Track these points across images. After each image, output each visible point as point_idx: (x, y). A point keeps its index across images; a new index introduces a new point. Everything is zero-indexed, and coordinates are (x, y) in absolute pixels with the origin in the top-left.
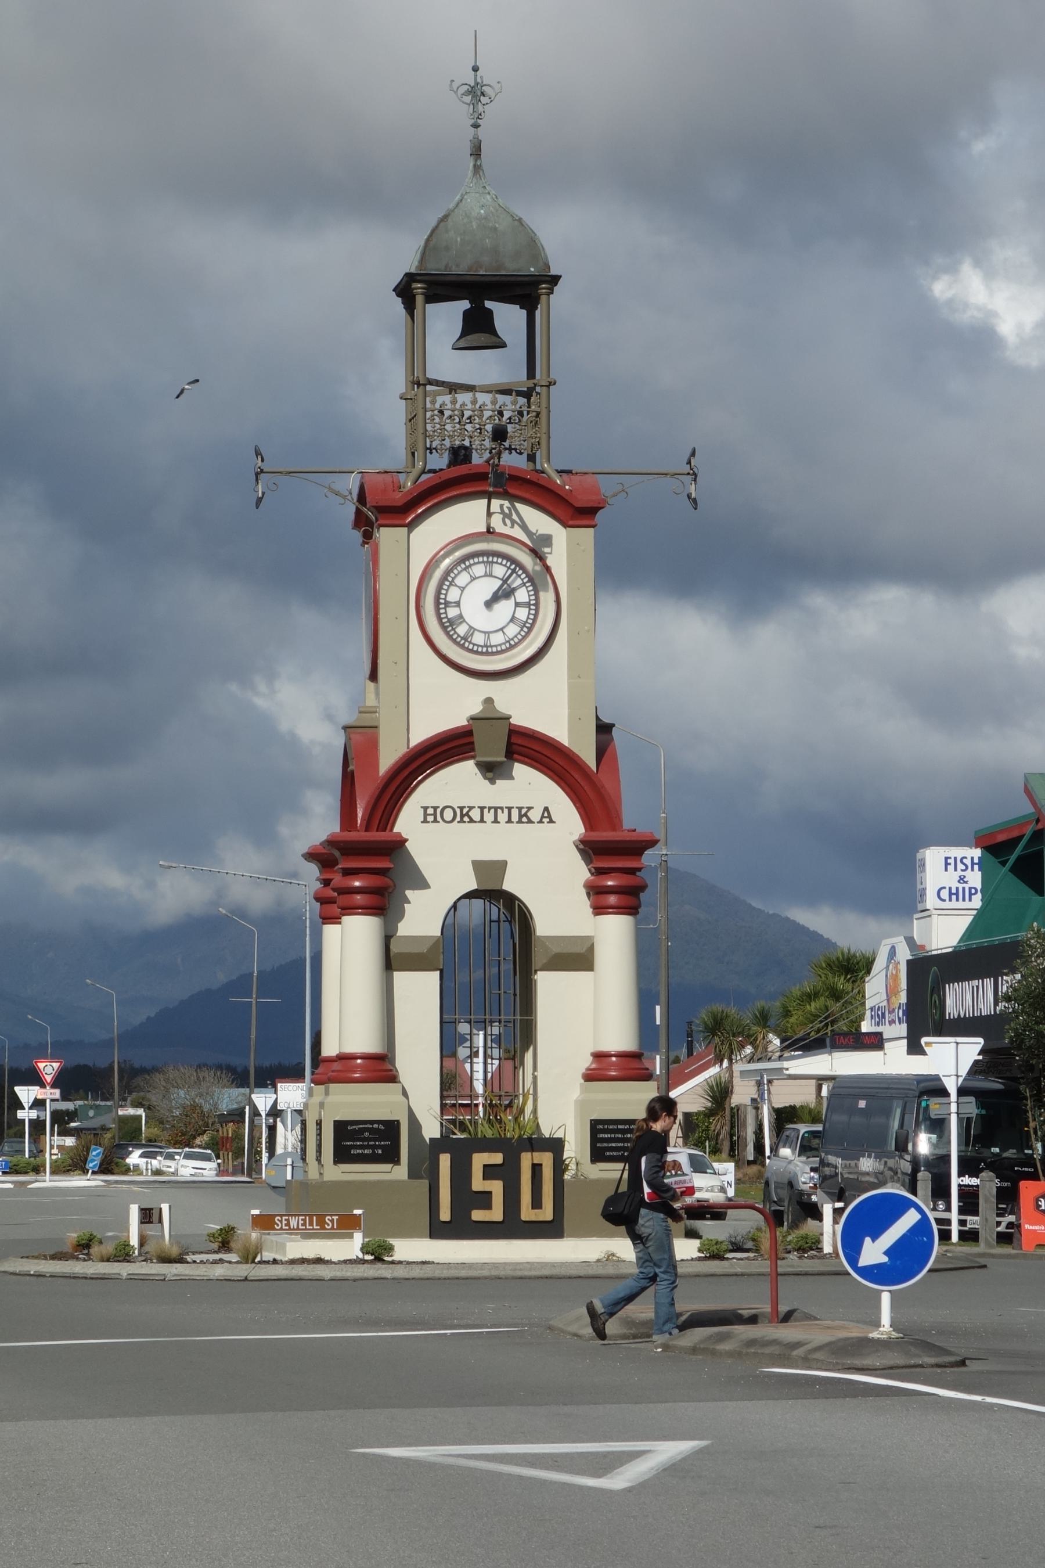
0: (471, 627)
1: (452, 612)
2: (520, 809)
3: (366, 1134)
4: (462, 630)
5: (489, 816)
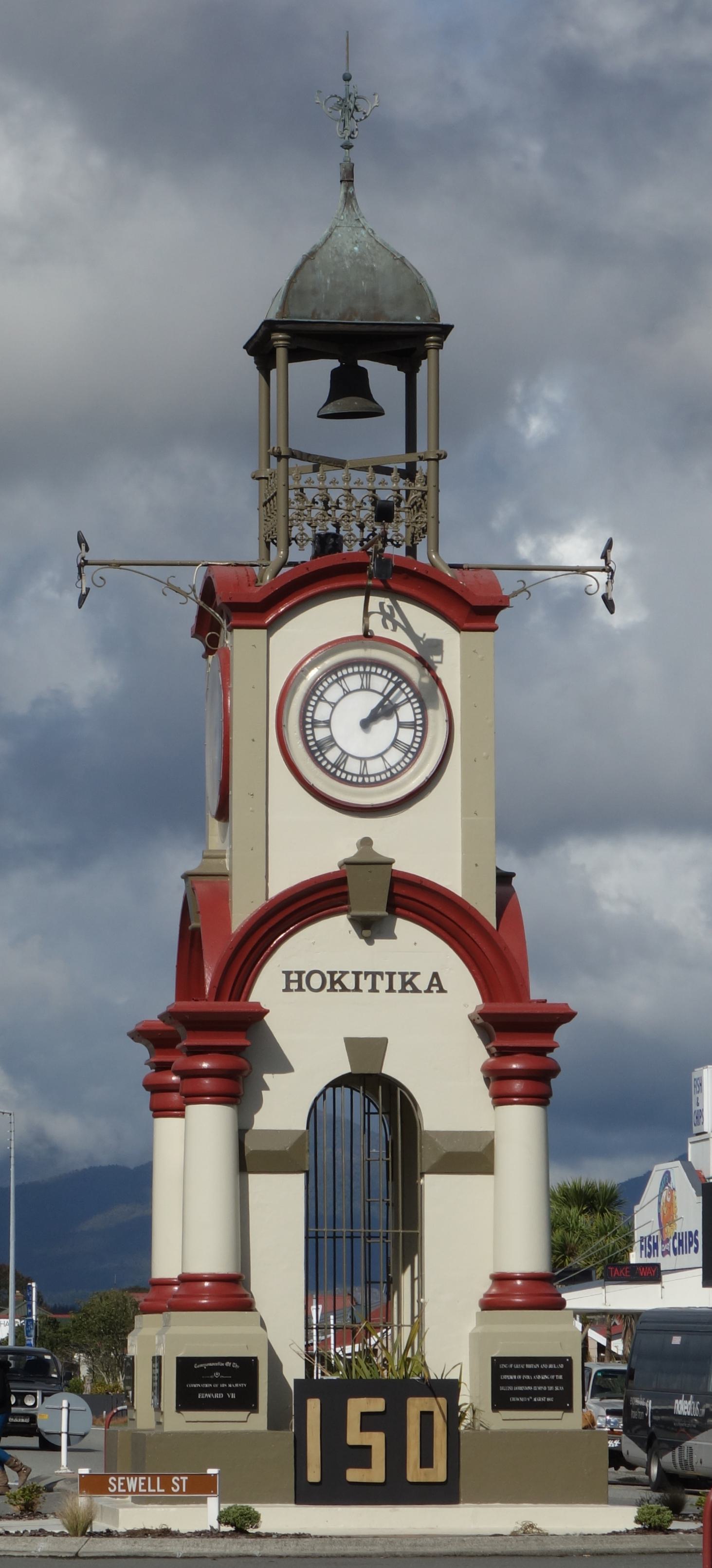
0: (343, 752)
1: (321, 734)
2: (403, 975)
3: (217, 1375)
4: (333, 755)
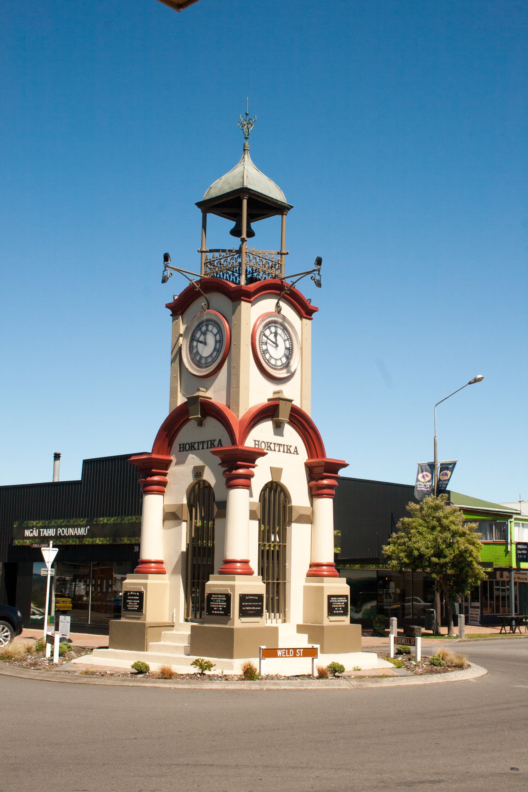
2: (211, 441)
5: (201, 446)
